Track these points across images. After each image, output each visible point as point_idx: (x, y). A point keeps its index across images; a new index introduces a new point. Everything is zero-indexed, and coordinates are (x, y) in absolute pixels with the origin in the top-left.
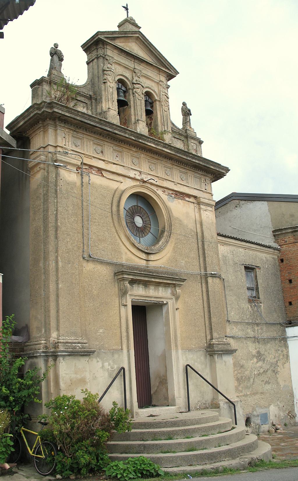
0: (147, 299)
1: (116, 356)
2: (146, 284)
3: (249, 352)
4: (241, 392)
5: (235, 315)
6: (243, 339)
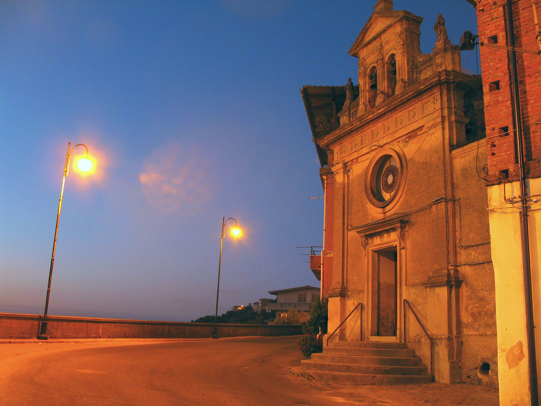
1: (361, 295)
2: (380, 234)
4: (478, 330)
5: (475, 236)
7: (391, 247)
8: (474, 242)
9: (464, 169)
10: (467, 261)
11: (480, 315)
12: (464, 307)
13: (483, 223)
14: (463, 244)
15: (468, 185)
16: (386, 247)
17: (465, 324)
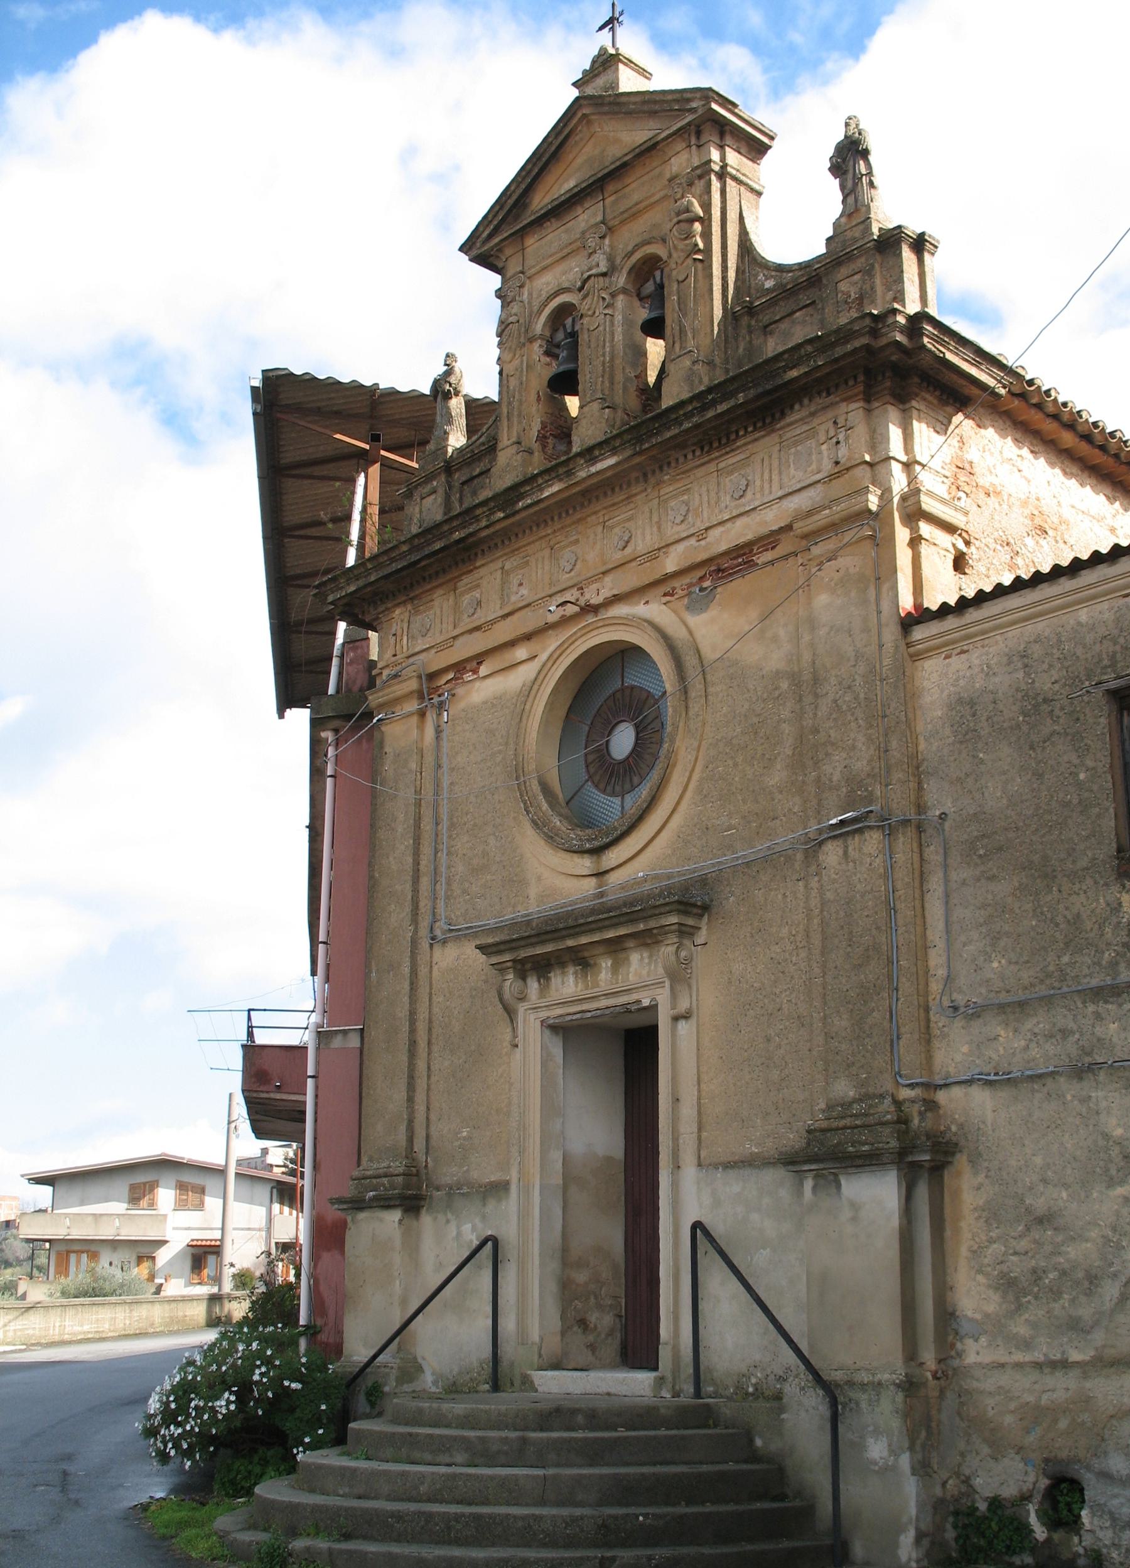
0: (585, 1007)
1: (491, 1205)
3: (1101, 1143)
4: (1026, 1345)
6: (1062, 1079)
7: (629, 1011)
8: (1008, 992)
9: (960, 701)
10: (977, 1066)
11: (1038, 1286)
12: (964, 1251)
13: (1049, 916)
14: (960, 999)
15: (982, 761)
16: (607, 1012)
17: (972, 1320)
